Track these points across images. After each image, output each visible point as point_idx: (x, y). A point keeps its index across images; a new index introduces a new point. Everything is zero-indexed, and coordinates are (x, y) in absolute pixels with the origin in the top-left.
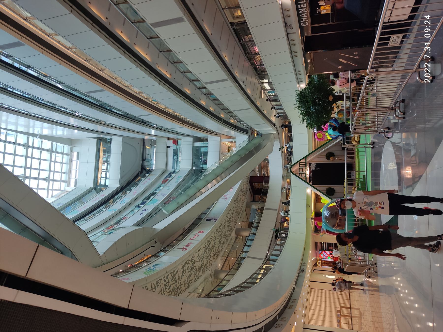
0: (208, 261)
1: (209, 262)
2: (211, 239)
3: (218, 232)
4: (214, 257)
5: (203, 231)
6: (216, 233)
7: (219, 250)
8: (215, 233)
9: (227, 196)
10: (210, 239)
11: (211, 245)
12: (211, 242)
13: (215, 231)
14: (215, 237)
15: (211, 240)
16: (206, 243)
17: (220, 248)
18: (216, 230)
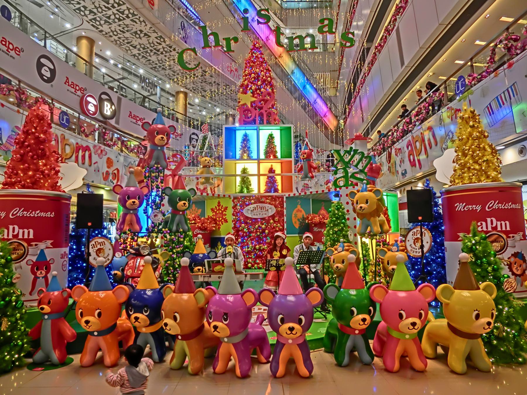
0: (95, 14)
1: (95, 19)
2: (139, 19)
3: (159, 41)
4: (111, 34)
5: (153, 5)
6: (156, 38)
7: (131, 48)
8: (157, 36)
9: (236, 73)
10: (137, 17)
11: (128, 21)
12: (132, 20)
13: (160, 34)
14: (149, 34)
15: (137, 21)
16: (124, 4)
17: (135, 52)
18: (161, 37)
